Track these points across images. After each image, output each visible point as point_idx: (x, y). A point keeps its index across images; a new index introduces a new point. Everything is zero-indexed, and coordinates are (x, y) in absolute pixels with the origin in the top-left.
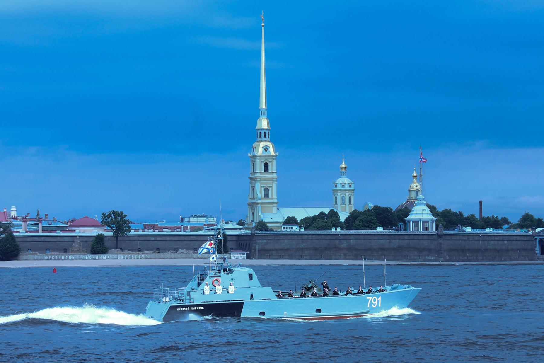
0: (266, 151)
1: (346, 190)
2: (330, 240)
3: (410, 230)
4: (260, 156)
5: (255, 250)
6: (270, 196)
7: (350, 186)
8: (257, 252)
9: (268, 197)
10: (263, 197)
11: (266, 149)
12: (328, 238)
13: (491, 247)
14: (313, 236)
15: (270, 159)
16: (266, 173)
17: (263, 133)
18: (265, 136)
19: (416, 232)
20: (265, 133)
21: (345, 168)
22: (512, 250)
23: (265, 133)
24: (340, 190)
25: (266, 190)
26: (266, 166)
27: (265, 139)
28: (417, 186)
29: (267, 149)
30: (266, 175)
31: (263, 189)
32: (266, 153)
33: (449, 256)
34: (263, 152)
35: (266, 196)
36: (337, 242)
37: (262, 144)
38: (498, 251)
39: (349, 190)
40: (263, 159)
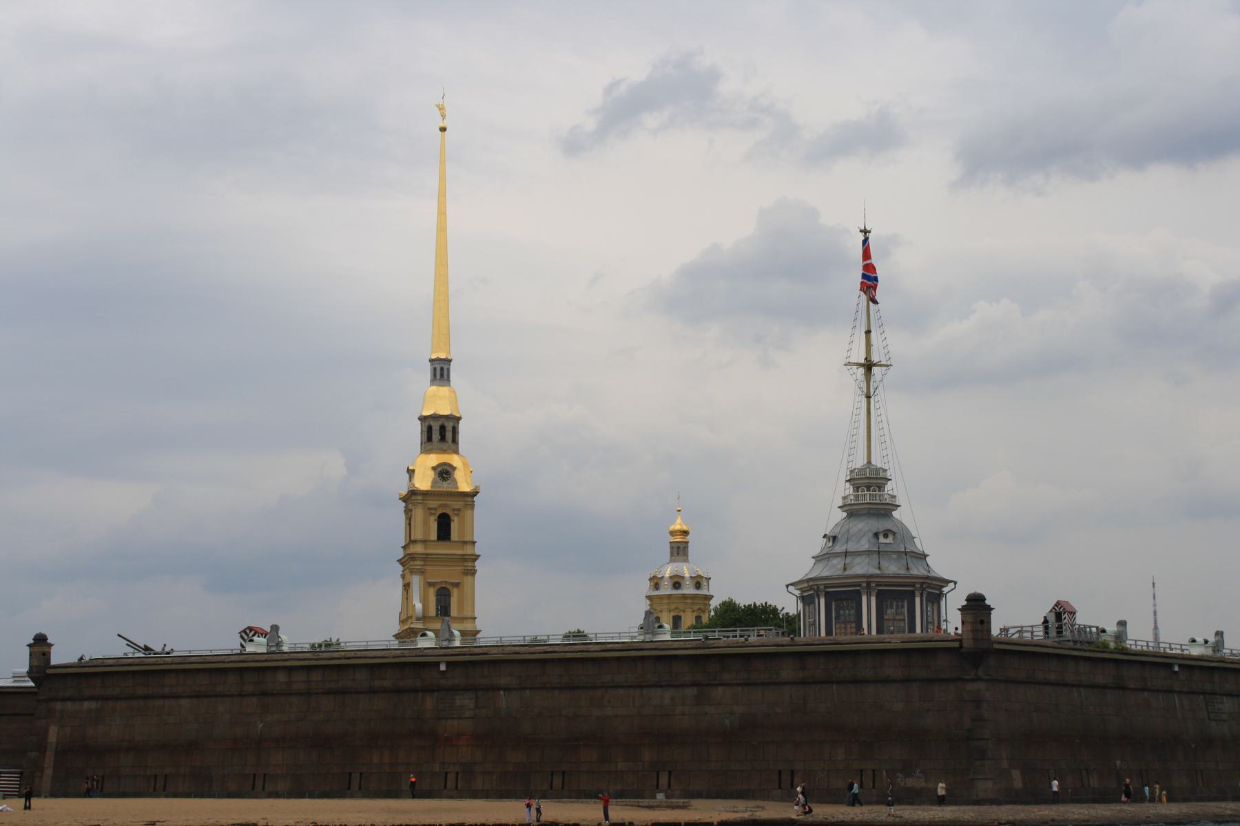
0: (444, 479)
1: (684, 597)
2: (398, 691)
4: (426, 494)
5: (41, 748)
7: (698, 585)
8: (49, 760)
11: (444, 472)
12: (387, 683)
14: (316, 676)
17: (436, 426)
20: (443, 428)
21: (685, 533)
23: (443, 428)
24: (670, 596)
27: (444, 446)
29: (447, 473)
30: (443, 549)
31: (432, 593)
32: (445, 487)
34: (434, 482)
36: (430, 702)
37: (434, 459)
39: (694, 597)
40: (433, 503)
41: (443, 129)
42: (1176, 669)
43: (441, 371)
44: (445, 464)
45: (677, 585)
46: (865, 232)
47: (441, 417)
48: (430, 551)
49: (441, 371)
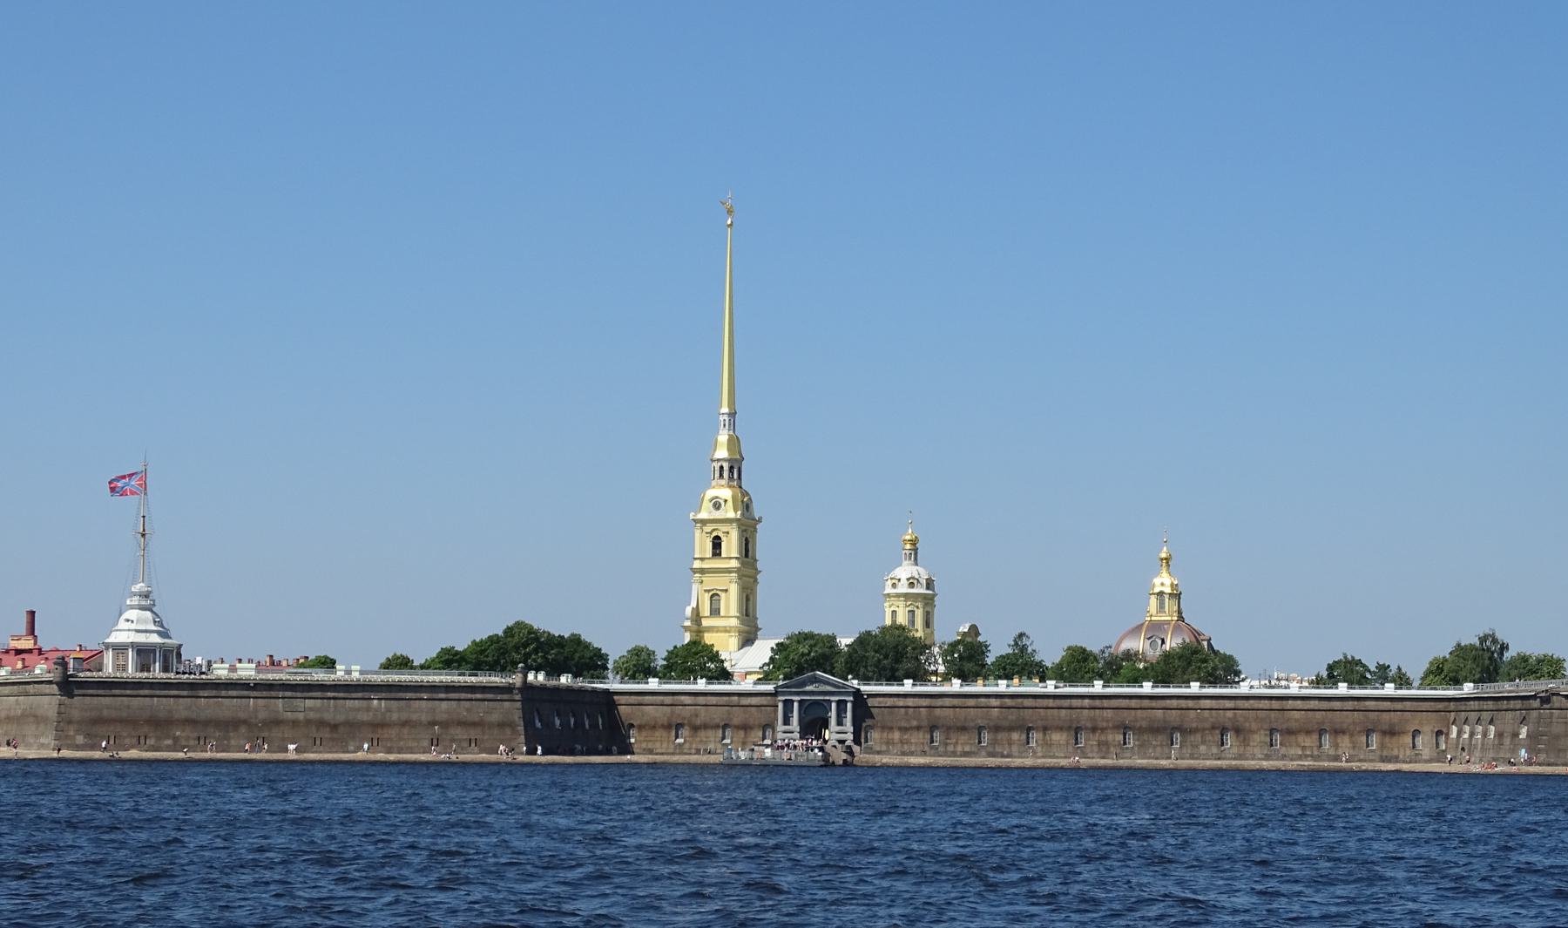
4: (704, 522)
7: (911, 585)
10: (706, 611)
13: (301, 716)
15: (724, 528)
18: (721, 475)
22: (405, 724)
25: (714, 597)
26: (717, 544)
27: (723, 482)
31: (707, 596)
33: (88, 735)
35: (715, 612)
38: (334, 727)
39: (906, 596)
40: (708, 528)
45: (894, 586)
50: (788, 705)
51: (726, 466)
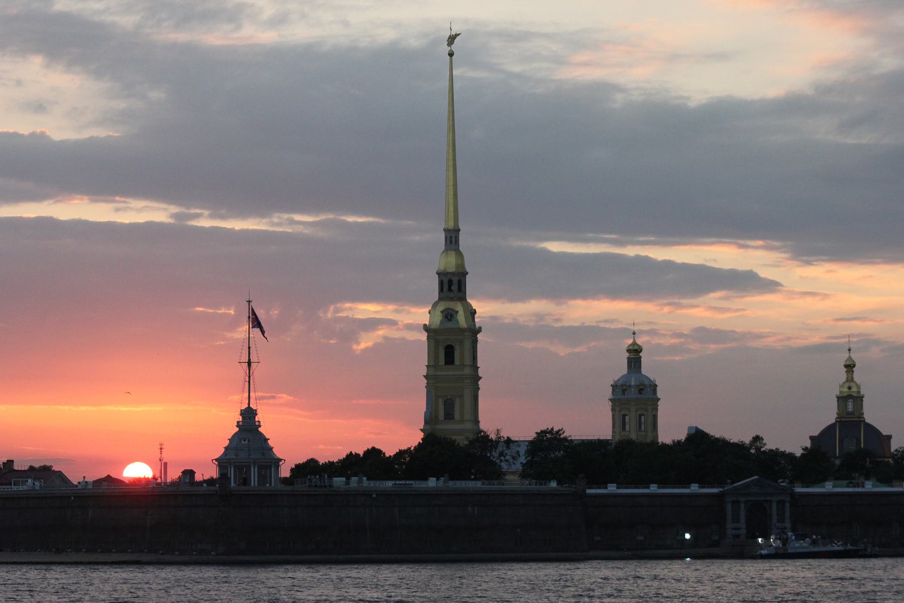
0: (450, 320)
3: (270, 484)
6: (457, 416)
7: (640, 391)
9: (453, 418)
10: (441, 416)
16: (450, 367)
19: (243, 488)
27: (452, 295)
28: (850, 388)
29: (451, 316)
30: (450, 372)
31: (441, 401)
32: (450, 325)
34: (442, 322)
35: (449, 416)
41: (451, 54)
42: (374, 496)
43: (452, 238)
44: (449, 309)
46: (249, 302)
47: (448, 273)
48: (439, 373)
49: (452, 238)
50: (736, 503)
51: (455, 280)
